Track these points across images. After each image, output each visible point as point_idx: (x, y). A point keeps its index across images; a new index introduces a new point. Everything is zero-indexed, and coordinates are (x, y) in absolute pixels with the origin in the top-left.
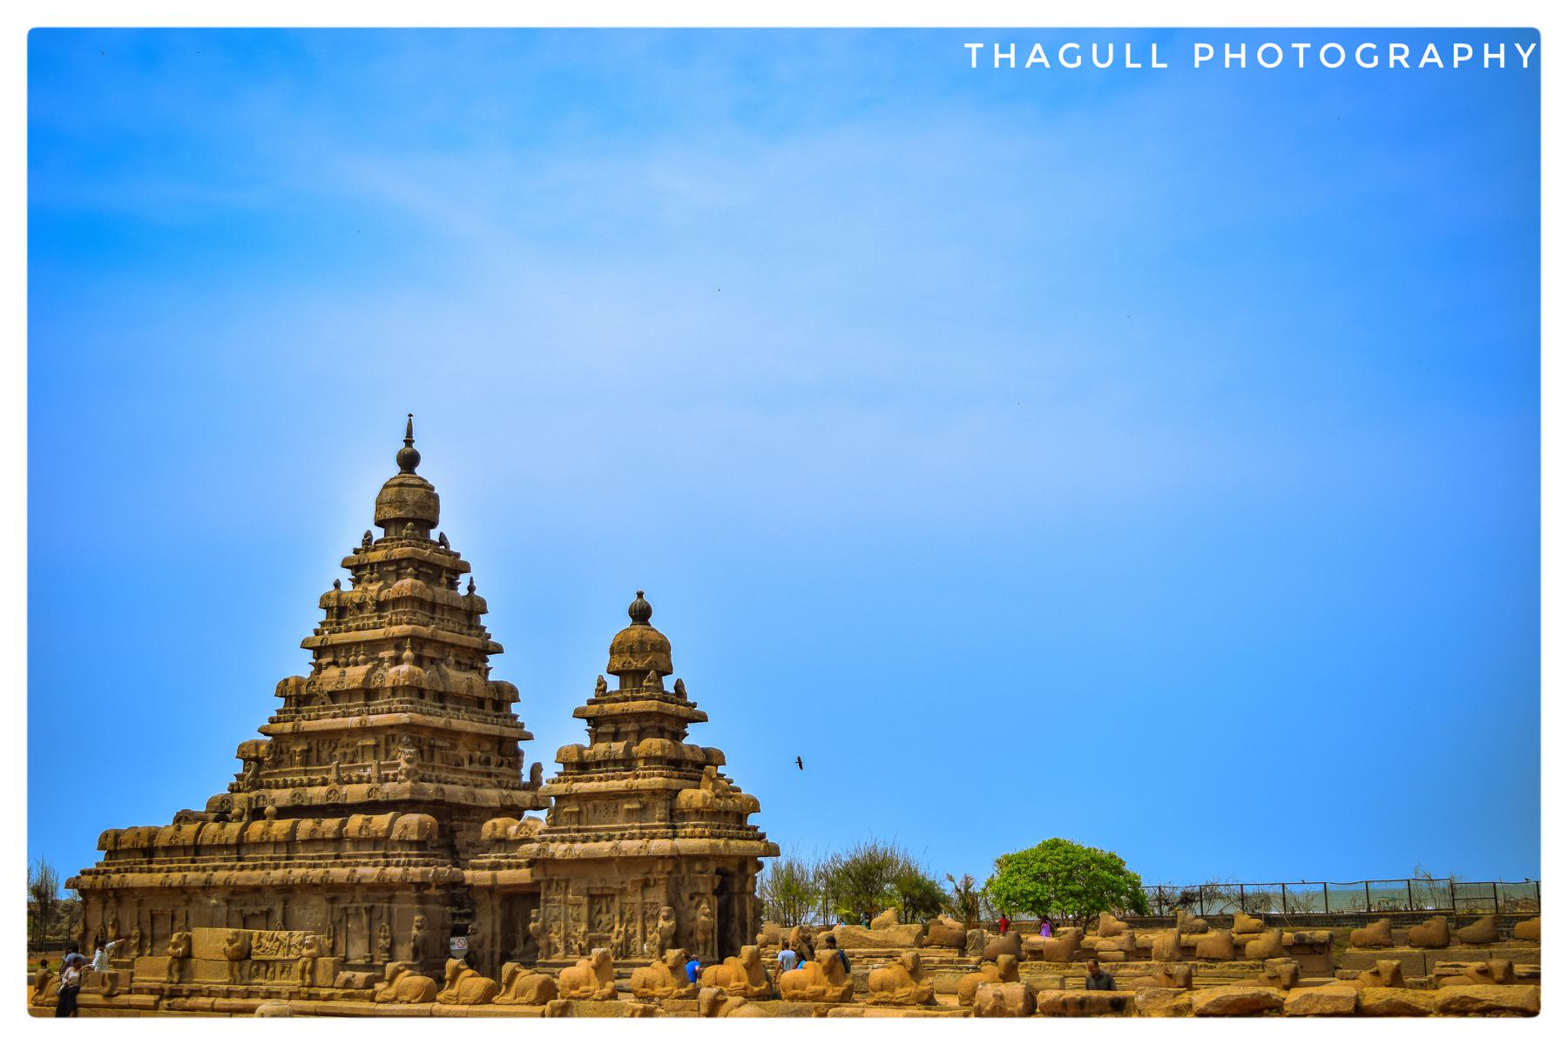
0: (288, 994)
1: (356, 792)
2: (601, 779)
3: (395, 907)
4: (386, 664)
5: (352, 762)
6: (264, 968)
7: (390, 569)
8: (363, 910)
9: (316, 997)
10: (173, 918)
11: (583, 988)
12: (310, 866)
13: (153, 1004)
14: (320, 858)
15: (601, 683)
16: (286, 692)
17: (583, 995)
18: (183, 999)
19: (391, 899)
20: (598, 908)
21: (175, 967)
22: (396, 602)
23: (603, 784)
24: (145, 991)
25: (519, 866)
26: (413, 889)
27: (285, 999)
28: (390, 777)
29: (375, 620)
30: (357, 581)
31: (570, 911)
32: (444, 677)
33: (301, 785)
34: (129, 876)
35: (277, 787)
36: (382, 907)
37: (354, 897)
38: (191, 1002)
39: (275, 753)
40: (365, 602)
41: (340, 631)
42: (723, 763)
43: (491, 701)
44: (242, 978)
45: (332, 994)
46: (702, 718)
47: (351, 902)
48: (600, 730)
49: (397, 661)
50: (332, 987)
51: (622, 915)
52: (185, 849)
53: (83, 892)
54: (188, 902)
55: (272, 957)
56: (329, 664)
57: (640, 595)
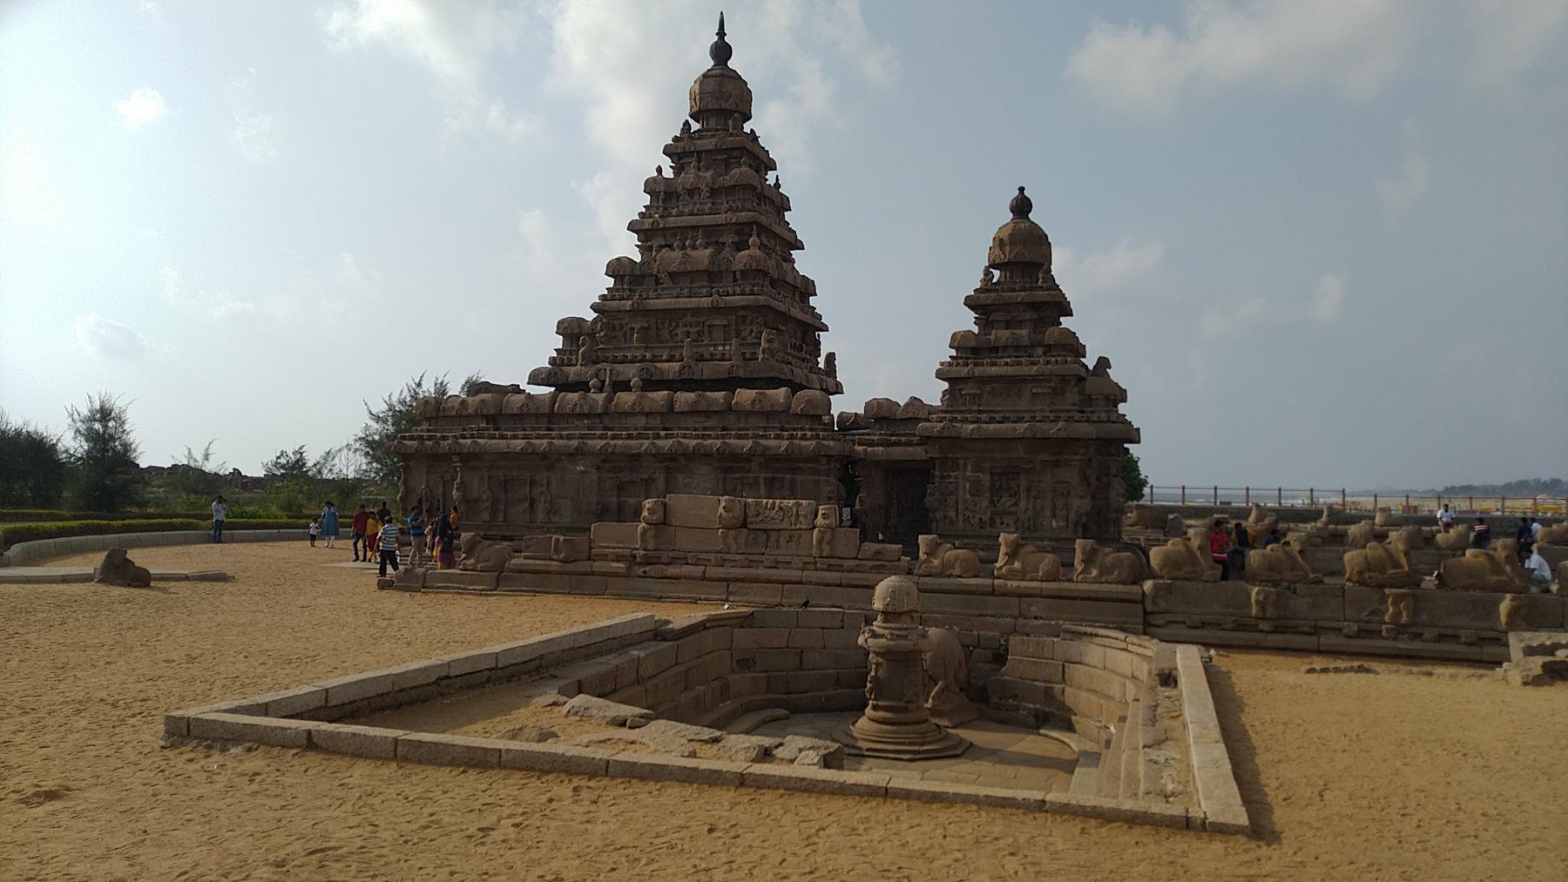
0: (800, 565)
2: (1007, 364)
3: (799, 478)
4: (727, 249)
5: (696, 341)
6: (764, 537)
7: (719, 157)
10: (532, 483)
12: (697, 437)
13: (624, 571)
14: (705, 429)
15: (987, 273)
17: (1188, 576)
18: (663, 566)
19: (793, 471)
21: (651, 533)
22: (732, 189)
23: (1009, 368)
24: (610, 557)
25: (909, 444)
27: (798, 569)
28: (747, 356)
29: (710, 205)
30: (678, 170)
31: (968, 487)
34: (481, 441)
35: (615, 361)
36: (783, 478)
38: (672, 570)
41: (670, 215)
42: (1084, 357)
45: (857, 566)
49: (741, 246)
50: (857, 558)
52: (538, 416)
54: (549, 468)
55: (776, 527)
56: (662, 247)
57: (1022, 189)
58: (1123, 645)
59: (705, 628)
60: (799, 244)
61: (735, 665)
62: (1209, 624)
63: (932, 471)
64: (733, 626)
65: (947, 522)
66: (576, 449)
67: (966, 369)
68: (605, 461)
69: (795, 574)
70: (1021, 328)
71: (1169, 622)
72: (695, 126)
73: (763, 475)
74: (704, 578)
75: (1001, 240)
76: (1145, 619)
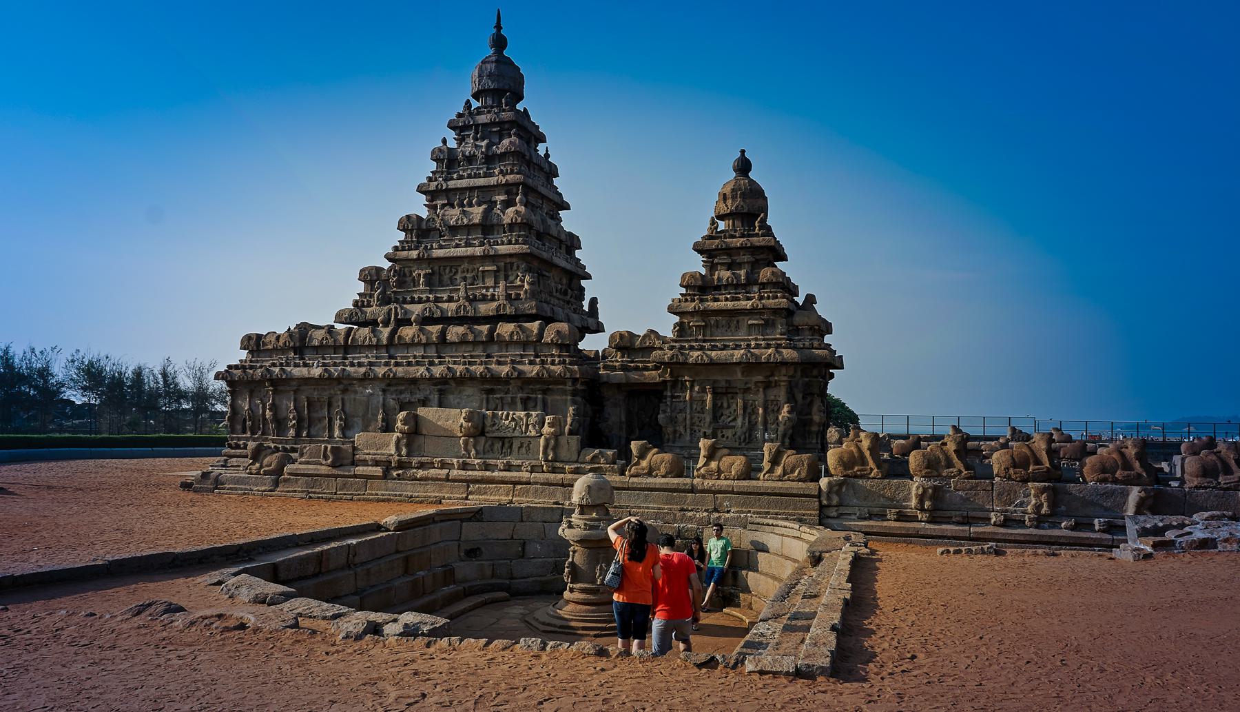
1: (485, 309)
2: (727, 299)
6: (498, 445)
7: (494, 130)
8: (519, 401)
9: (562, 471)
11: (856, 468)
14: (472, 357)
15: (713, 223)
16: (408, 227)
18: (415, 470)
20: (719, 405)
22: (503, 156)
23: (729, 303)
26: (570, 384)
29: (485, 169)
30: (461, 141)
32: (543, 221)
33: (428, 300)
37: (509, 389)
38: (420, 473)
39: (399, 275)
40: (474, 155)
41: (452, 179)
42: (798, 296)
43: (565, 246)
44: (477, 453)
45: (578, 468)
46: (783, 258)
47: (506, 394)
48: (716, 261)
49: (508, 204)
50: (577, 462)
51: (745, 408)
52: (336, 348)
53: (229, 383)
55: (509, 435)
56: (443, 206)
58: (797, 534)
59: (434, 522)
60: (565, 205)
61: (462, 554)
62: (876, 515)
63: (665, 394)
64: (462, 521)
65: (678, 435)
66: (365, 374)
67: (693, 304)
68: (389, 385)
69: (525, 475)
70: (740, 269)
71: (842, 514)
72: (475, 104)
73: (520, 395)
74: (447, 479)
75: (725, 195)
76: (820, 511)
